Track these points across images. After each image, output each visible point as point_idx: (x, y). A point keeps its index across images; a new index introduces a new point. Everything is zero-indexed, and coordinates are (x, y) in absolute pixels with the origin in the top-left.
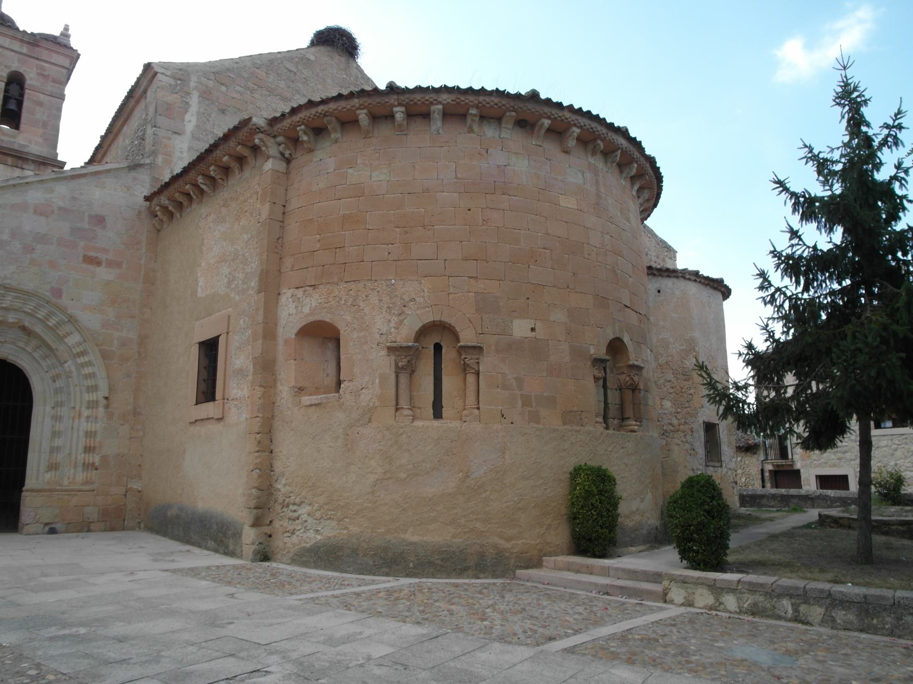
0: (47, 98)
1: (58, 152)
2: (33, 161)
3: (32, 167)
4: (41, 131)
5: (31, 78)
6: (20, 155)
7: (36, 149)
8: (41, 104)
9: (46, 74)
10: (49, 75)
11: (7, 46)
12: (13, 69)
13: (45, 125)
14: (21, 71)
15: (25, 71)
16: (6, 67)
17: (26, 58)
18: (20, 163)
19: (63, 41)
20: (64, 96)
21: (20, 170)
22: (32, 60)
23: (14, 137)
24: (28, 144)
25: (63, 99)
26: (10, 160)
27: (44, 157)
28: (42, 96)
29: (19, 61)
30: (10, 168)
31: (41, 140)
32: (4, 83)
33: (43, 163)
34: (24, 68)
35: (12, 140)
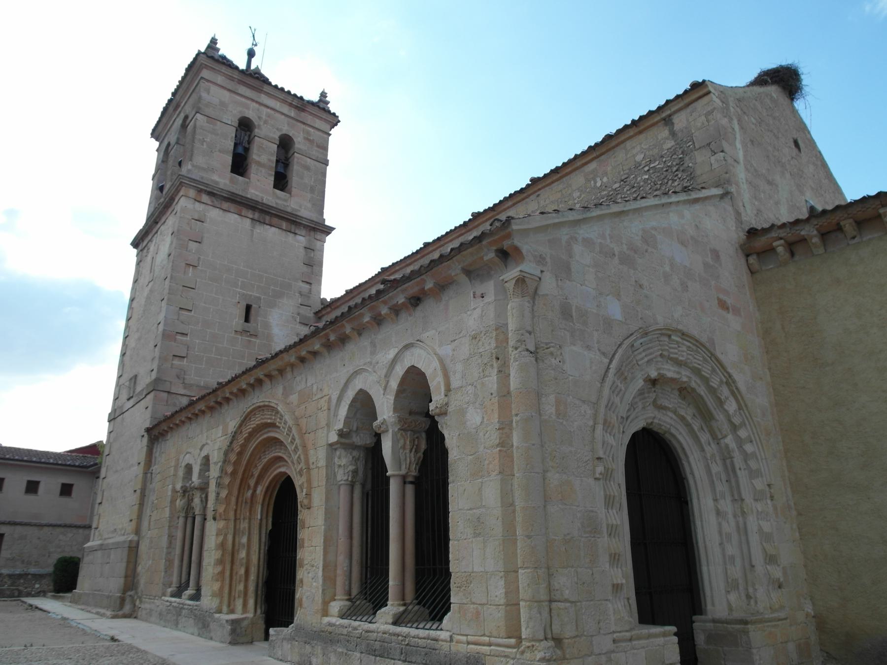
0: (313, 162)
1: (324, 217)
2: (305, 227)
3: (303, 232)
4: (309, 195)
5: (299, 142)
6: (295, 219)
7: (306, 213)
8: (307, 168)
9: (312, 138)
10: (313, 140)
11: (278, 109)
12: (284, 132)
13: (312, 190)
14: (291, 135)
15: (293, 134)
16: (277, 129)
17: (294, 122)
18: (293, 228)
19: (322, 105)
20: (328, 161)
21: (293, 235)
22: (299, 124)
23: (286, 200)
24: (299, 209)
25: (327, 165)
26: (284, 225)
27: (316, 222)
28: (309, 160)
29: (288, 124)
30: (284, 232)
31: (309, 205)
32: (276, 146)
33: (314, 228)
34: (293, 132)
35: (285, 203)
